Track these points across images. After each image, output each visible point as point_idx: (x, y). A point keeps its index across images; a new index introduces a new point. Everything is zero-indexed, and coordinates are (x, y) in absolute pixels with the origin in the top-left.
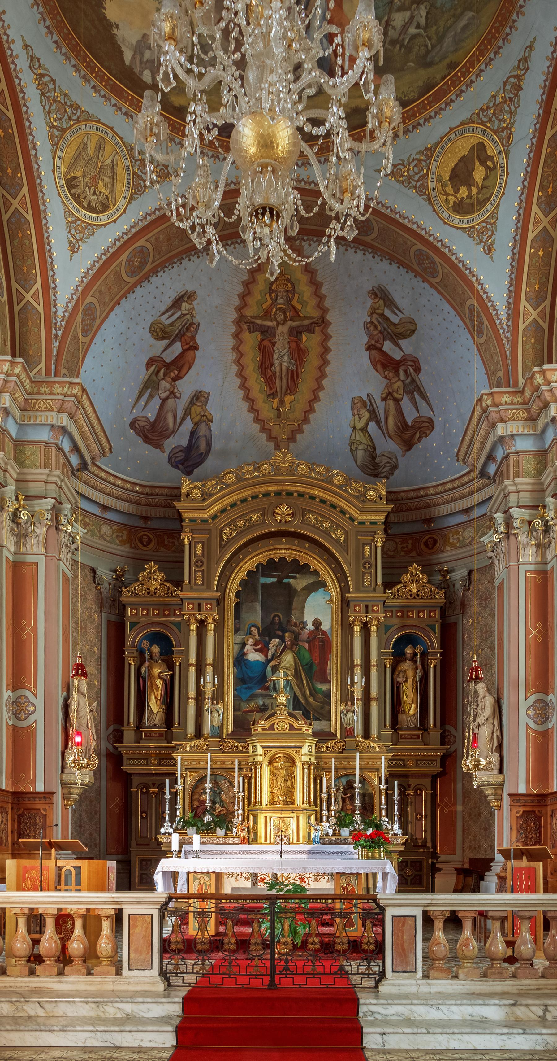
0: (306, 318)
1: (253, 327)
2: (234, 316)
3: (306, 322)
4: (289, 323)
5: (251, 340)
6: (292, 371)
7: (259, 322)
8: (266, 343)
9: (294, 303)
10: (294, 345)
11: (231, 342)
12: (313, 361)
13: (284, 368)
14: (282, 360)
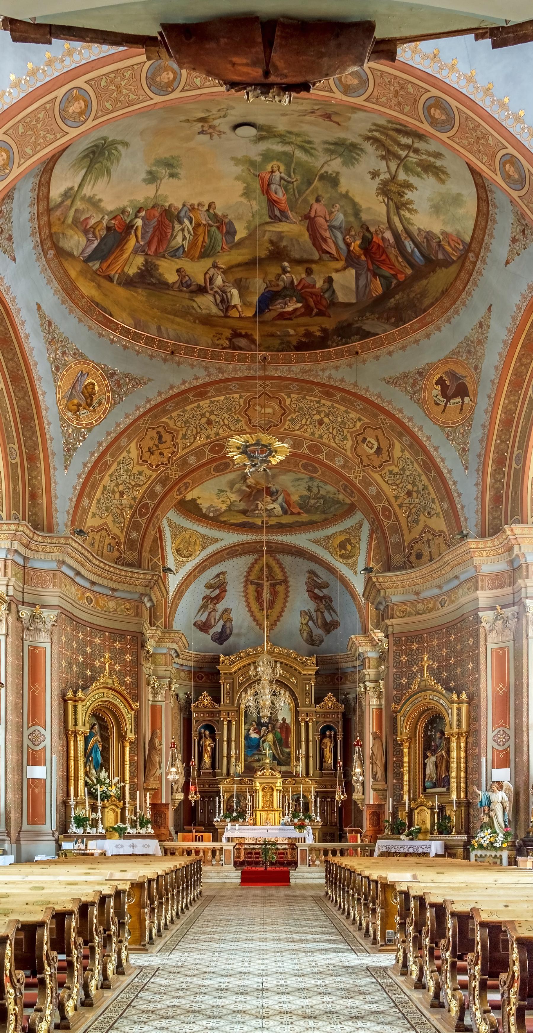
12: (281, 595)
14: (266, 594)
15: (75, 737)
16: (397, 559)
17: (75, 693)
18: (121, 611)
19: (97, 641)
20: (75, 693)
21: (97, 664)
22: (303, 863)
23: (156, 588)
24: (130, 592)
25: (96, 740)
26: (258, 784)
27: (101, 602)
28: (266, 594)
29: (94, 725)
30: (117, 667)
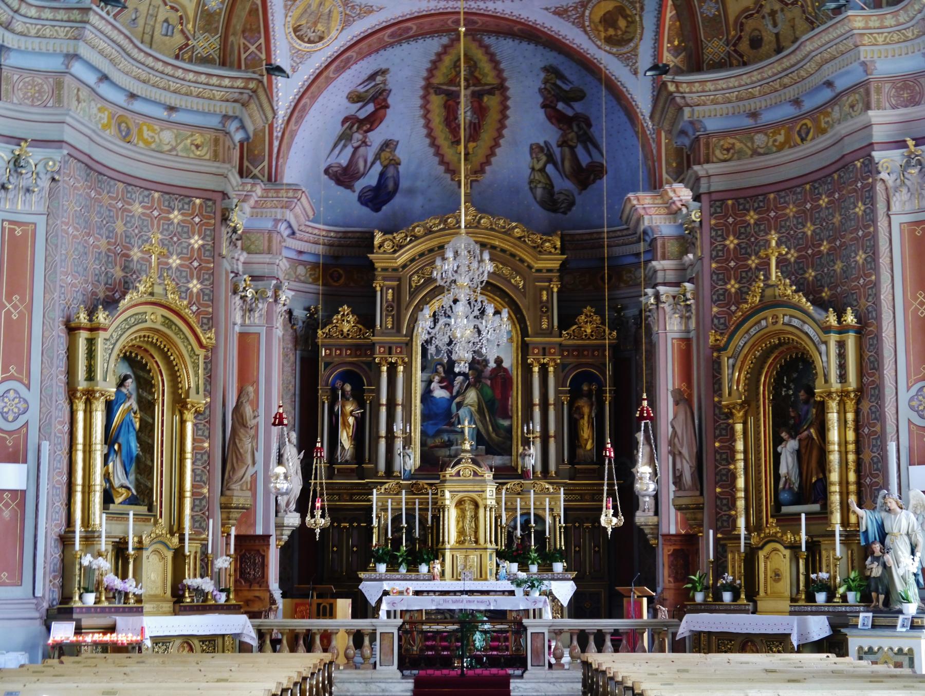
0: (486, 84)
1: (438, 91)
2: (423, 83)
3: (487, 87)
4: (472, 88)
5: (437, 101)
6: (475, 124)
7: (445, 87)
8: (450, 102)
9: (476, 74)
10: (476, 104)
11: (419, 102)
13: (467, 121)
14: (464, 114)
15: (88, 402)
16: (714, 48)
17: (91, 313)
18: (186, 149)
19: (137, 209)
20: (91, 313)
21: (136, 254)
22: (538, 664)
23: (253, 106)
24: (203, 113)
25: (130, 409)
26: (447, 495)
27: (146, 134)
28: (464, 114)
29: (126, 378)
30: (174, 261)
